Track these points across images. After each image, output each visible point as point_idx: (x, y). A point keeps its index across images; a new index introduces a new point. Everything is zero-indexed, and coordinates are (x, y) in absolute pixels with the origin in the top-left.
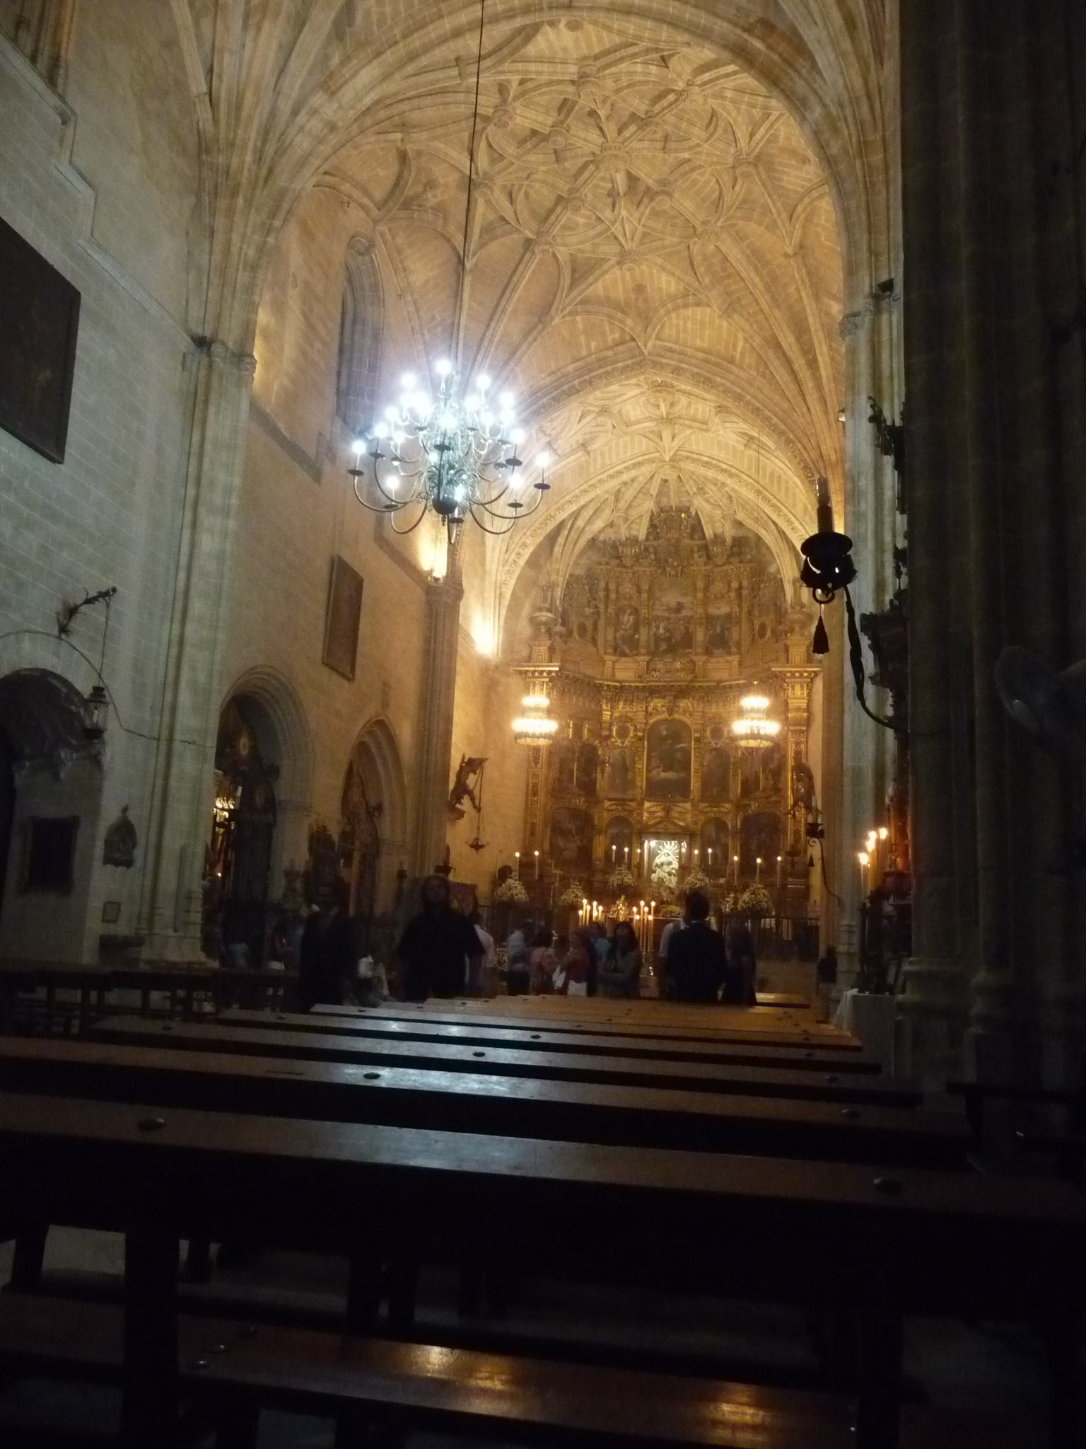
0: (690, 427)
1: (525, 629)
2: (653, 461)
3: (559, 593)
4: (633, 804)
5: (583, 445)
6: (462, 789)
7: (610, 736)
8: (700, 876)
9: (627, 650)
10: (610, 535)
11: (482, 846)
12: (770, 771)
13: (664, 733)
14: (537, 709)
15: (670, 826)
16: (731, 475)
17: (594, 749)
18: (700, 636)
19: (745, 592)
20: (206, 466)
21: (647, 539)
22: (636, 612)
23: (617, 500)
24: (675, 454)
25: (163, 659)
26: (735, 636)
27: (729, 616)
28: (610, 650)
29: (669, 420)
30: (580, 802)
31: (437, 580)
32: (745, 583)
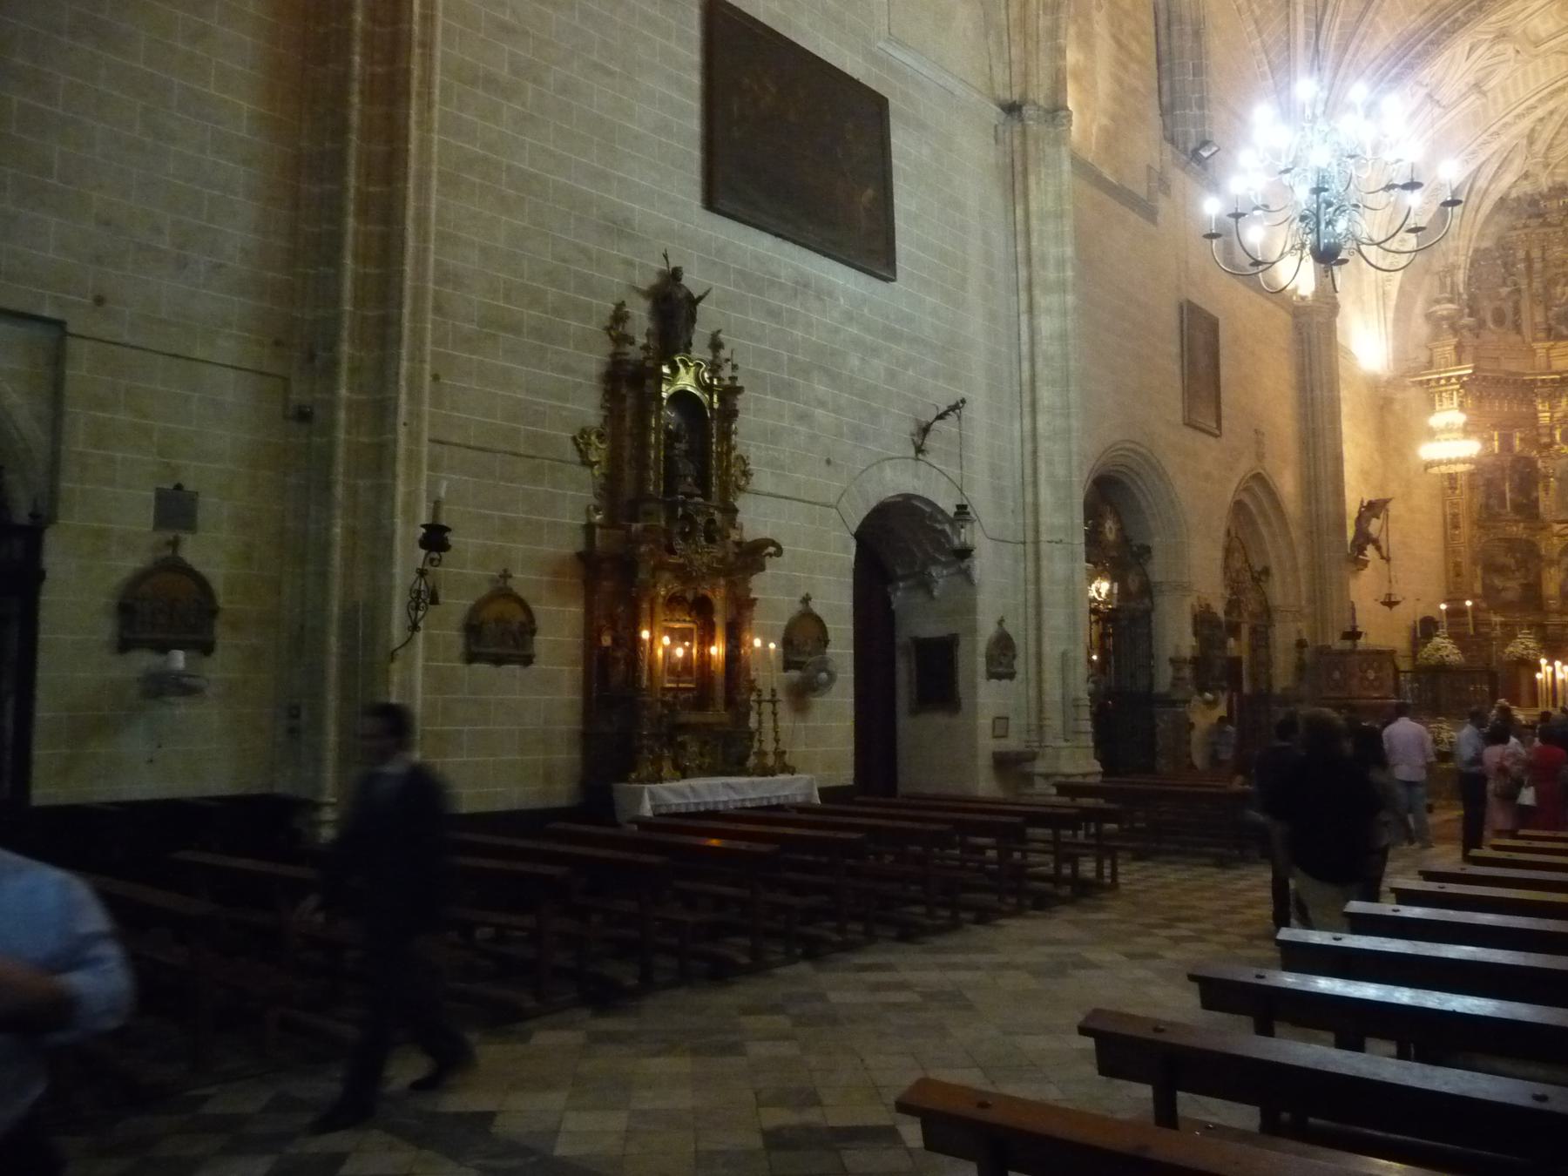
1: (1421, 329)
3: (1461, 276)
5: (1477, 86)
6: (1364, 538)
7: (1552, 443)
10: (1527, 187)
11: (1397, 603)
14: (1449, 429)
17: (1530, 462)
20: (1034, 243)
25: (1018, 457)
28: (1541, 335)
30: (1518, 530)
31: (1303, 298)
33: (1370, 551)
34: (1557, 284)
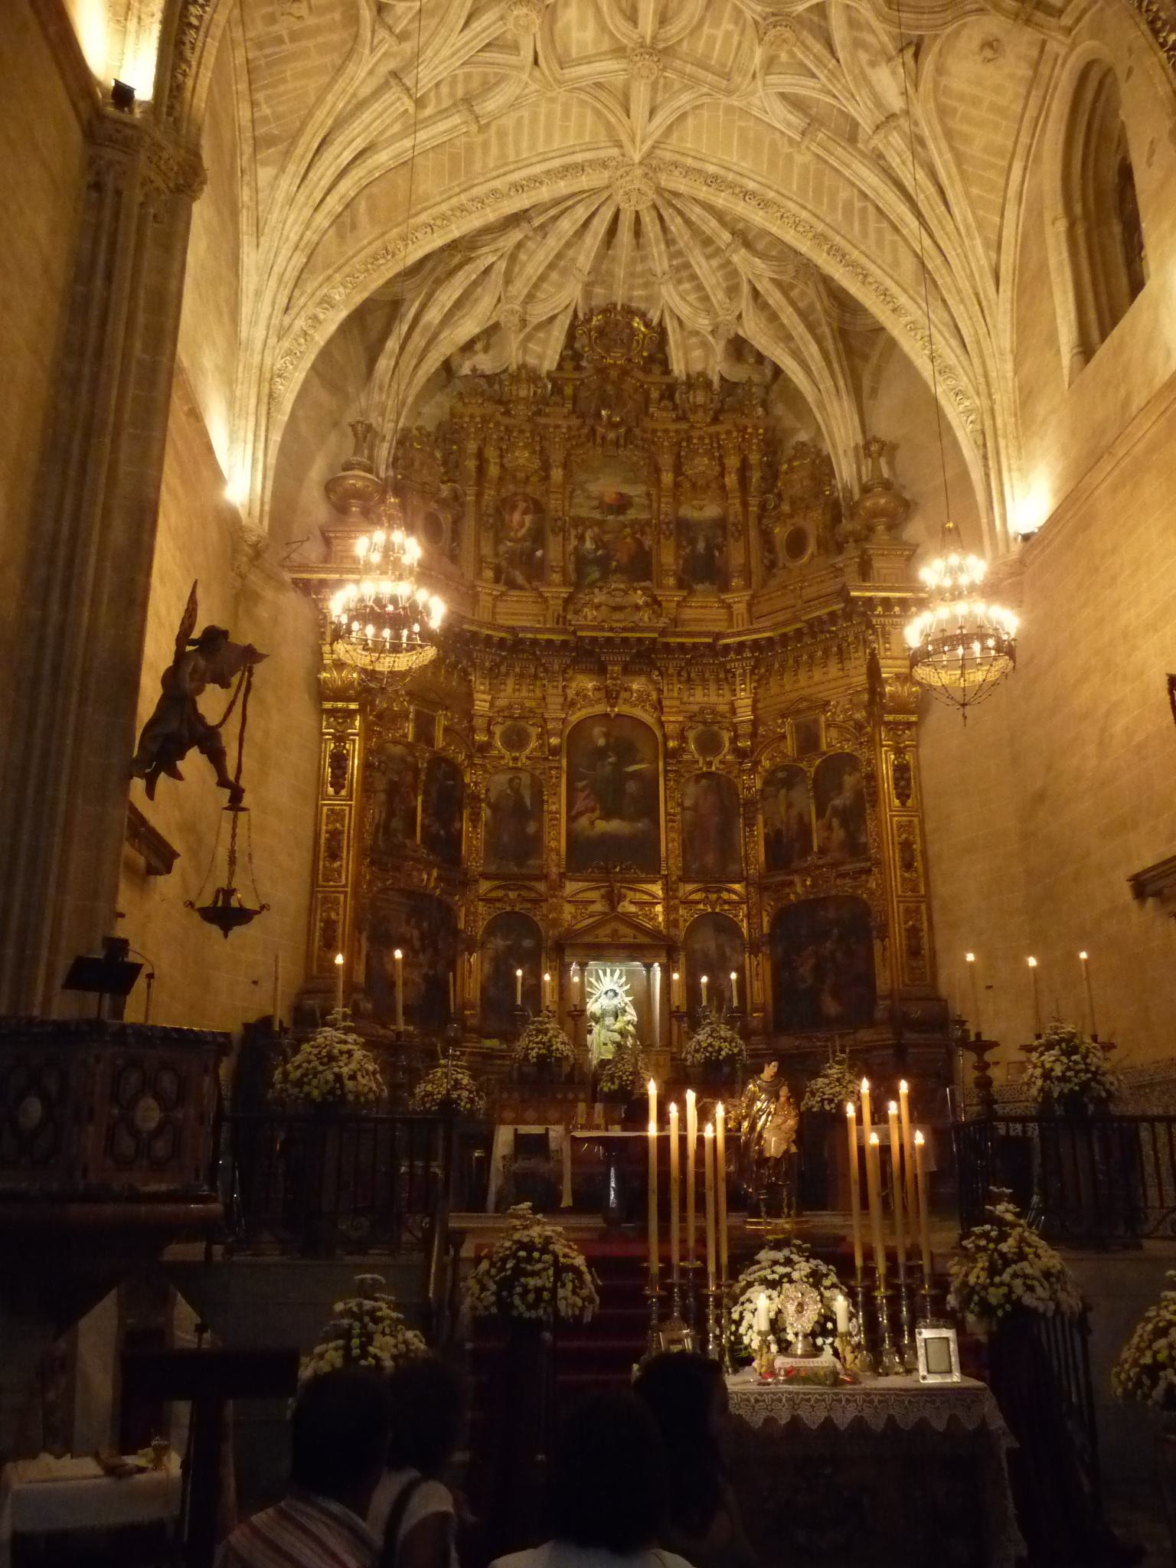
0: (693, 82)
2: (604, 164)
3: (384, 452)
4: (542, 887)
8: (725, 1032)
9: (520, 579)
10: (485, 362)
11: (243, 916)
12: (836, 812)
13: (601, 742)
15: (624, 930)
16: (764, 204)
18: (668, 557)
19: (755, 476)
21: (560, 367)
22: (537, 507)
23: (508, 280)
24: (649, 154)
26: (737, 559)
27: (721, 523)
28: (489, 574)
29: (661, 52)
30: (428, 879)
32: (754, 458)
33: (193, 763)
34: (514, 508)
